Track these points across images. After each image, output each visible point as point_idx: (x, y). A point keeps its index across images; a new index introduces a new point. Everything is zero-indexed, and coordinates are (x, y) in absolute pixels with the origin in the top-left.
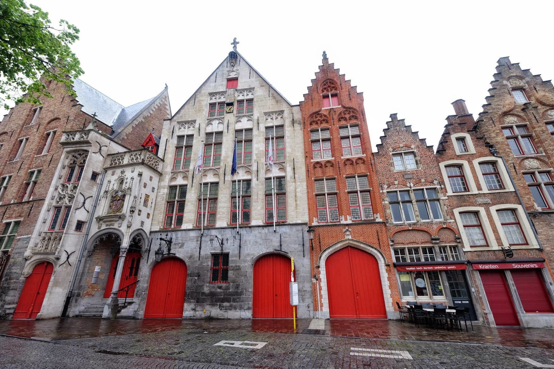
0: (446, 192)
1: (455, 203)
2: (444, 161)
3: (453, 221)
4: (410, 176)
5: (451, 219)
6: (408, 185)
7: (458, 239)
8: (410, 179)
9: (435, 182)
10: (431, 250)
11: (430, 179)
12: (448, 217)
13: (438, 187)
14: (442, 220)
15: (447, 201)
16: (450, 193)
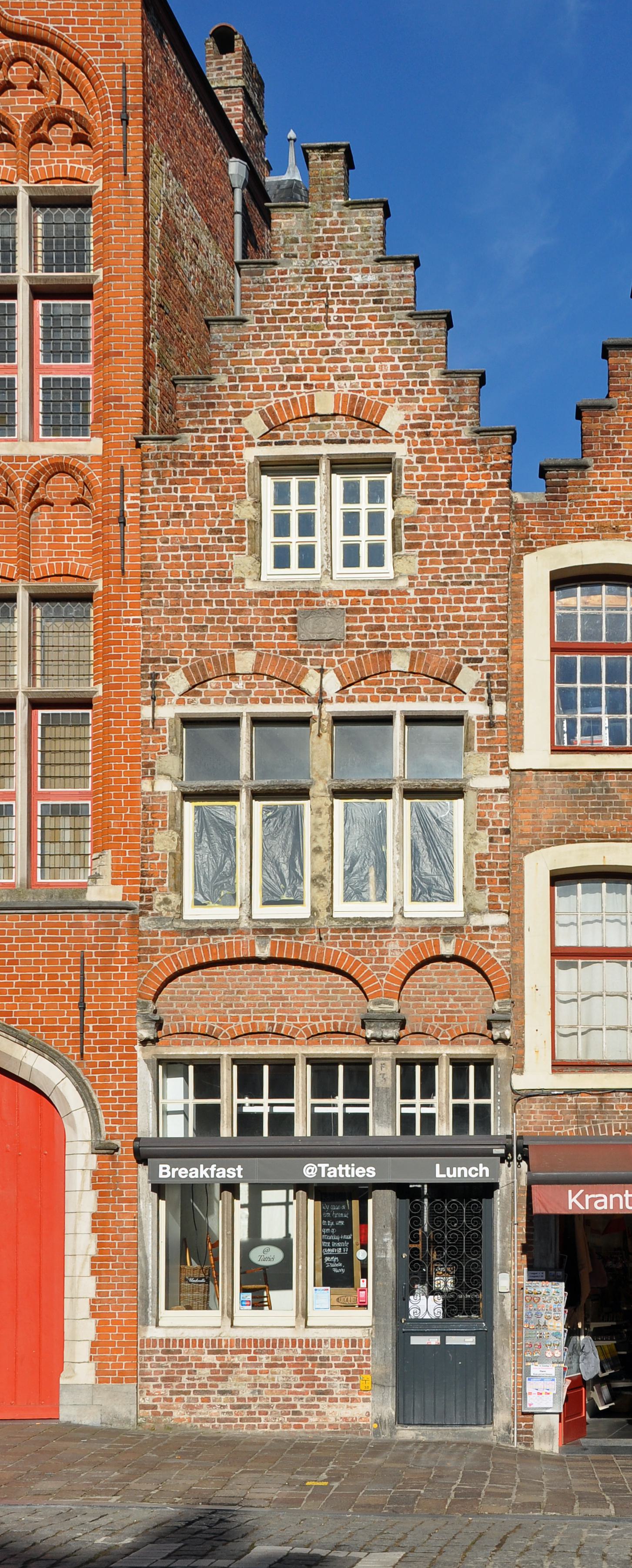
0: (519, 746)
1: (547, 815)
2: (561, 539)
3: (502, 919)
4: (331, 628)
5: (494, 908)
6: (311, 684)
7: (503, 1026)
8: (331, 642)
9: (468, 678)
10: (358, 1073)
11: (441, 654)
12: (482, 900)
13: (475, 710)
14: (451, 910)
15: (502, 799)
16: (536, 752)
